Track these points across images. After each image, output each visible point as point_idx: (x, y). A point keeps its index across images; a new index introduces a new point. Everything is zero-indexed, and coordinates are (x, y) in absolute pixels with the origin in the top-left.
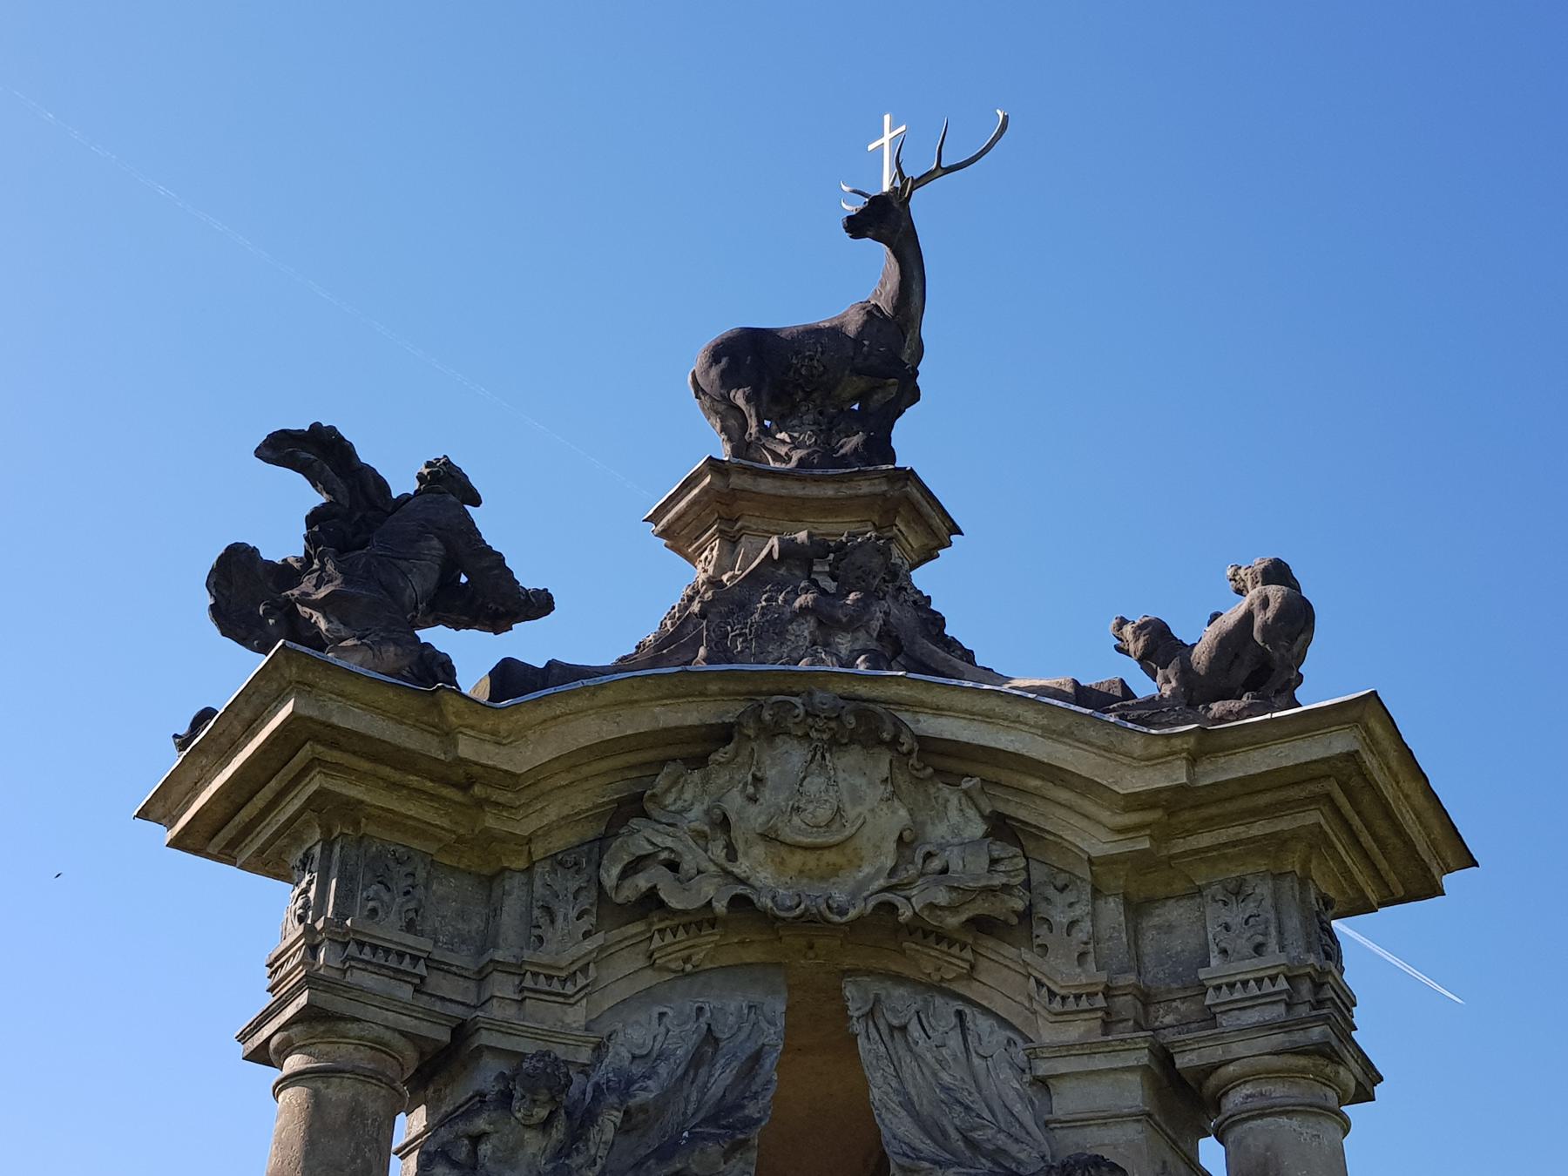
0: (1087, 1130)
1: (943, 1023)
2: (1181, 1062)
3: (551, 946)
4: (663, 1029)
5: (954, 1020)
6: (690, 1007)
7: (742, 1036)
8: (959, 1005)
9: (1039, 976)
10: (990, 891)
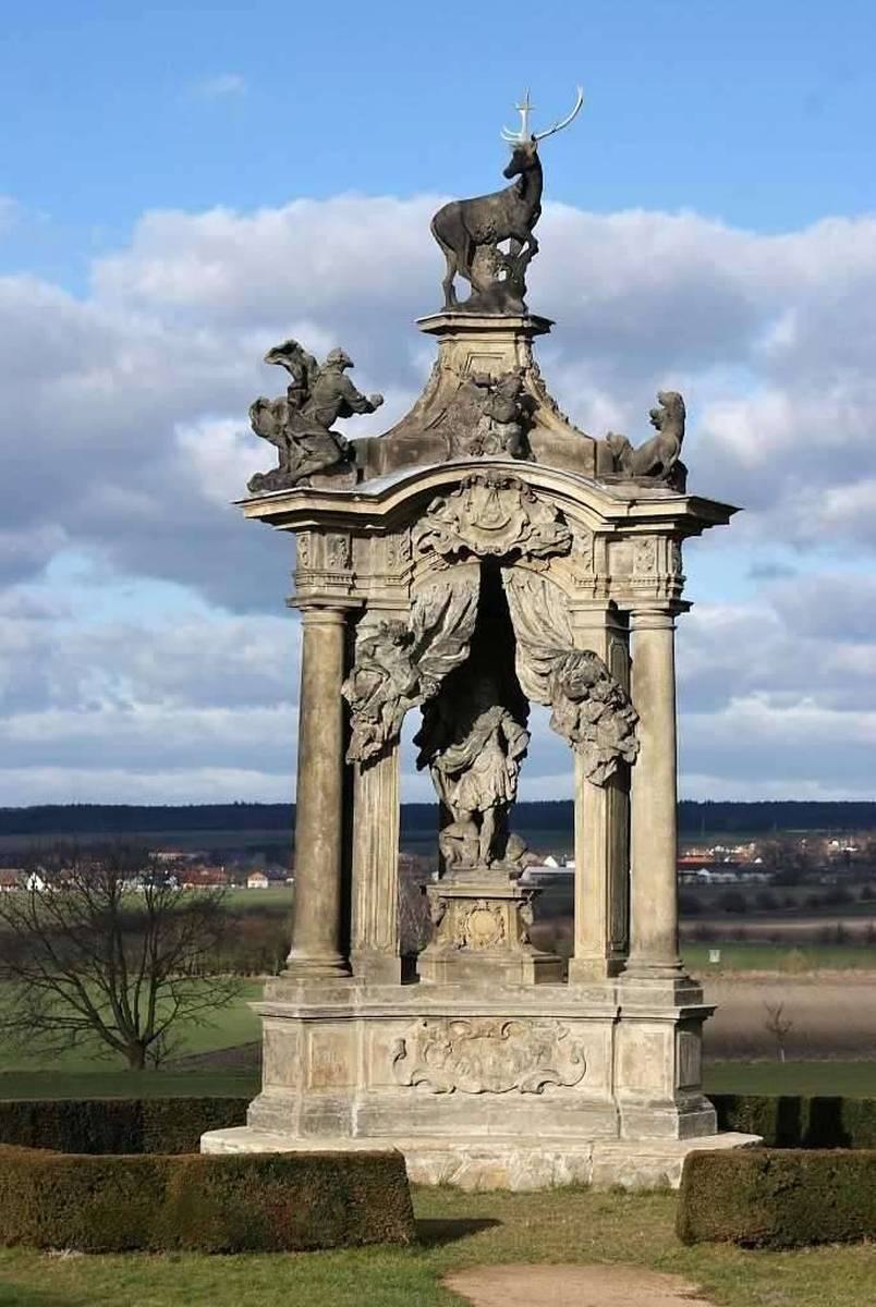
5: (540, 585)
6: (445, 583)
8: (542, 579)
10: (555, 544)
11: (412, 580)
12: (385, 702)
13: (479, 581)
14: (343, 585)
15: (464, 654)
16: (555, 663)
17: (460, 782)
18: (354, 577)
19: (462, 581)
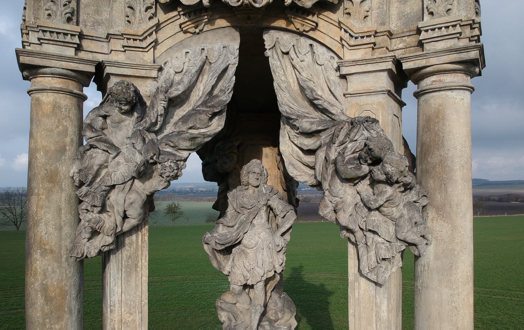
0: (361, 97)
1: (304, 50)
2: (406, 66)
3: (135, 25)
4: (187, 60)
5: (309, 49)
6: (198, 48)
7: (220, 61)
9: (346, 28)
11: (156, 42)
12: (113, 187)
13: (238, 47)
14: (65, 44)
15: (217, 125)
16: (324, 137)
17: (231, 256)
18: (81, 36)
19: (217, 46)
